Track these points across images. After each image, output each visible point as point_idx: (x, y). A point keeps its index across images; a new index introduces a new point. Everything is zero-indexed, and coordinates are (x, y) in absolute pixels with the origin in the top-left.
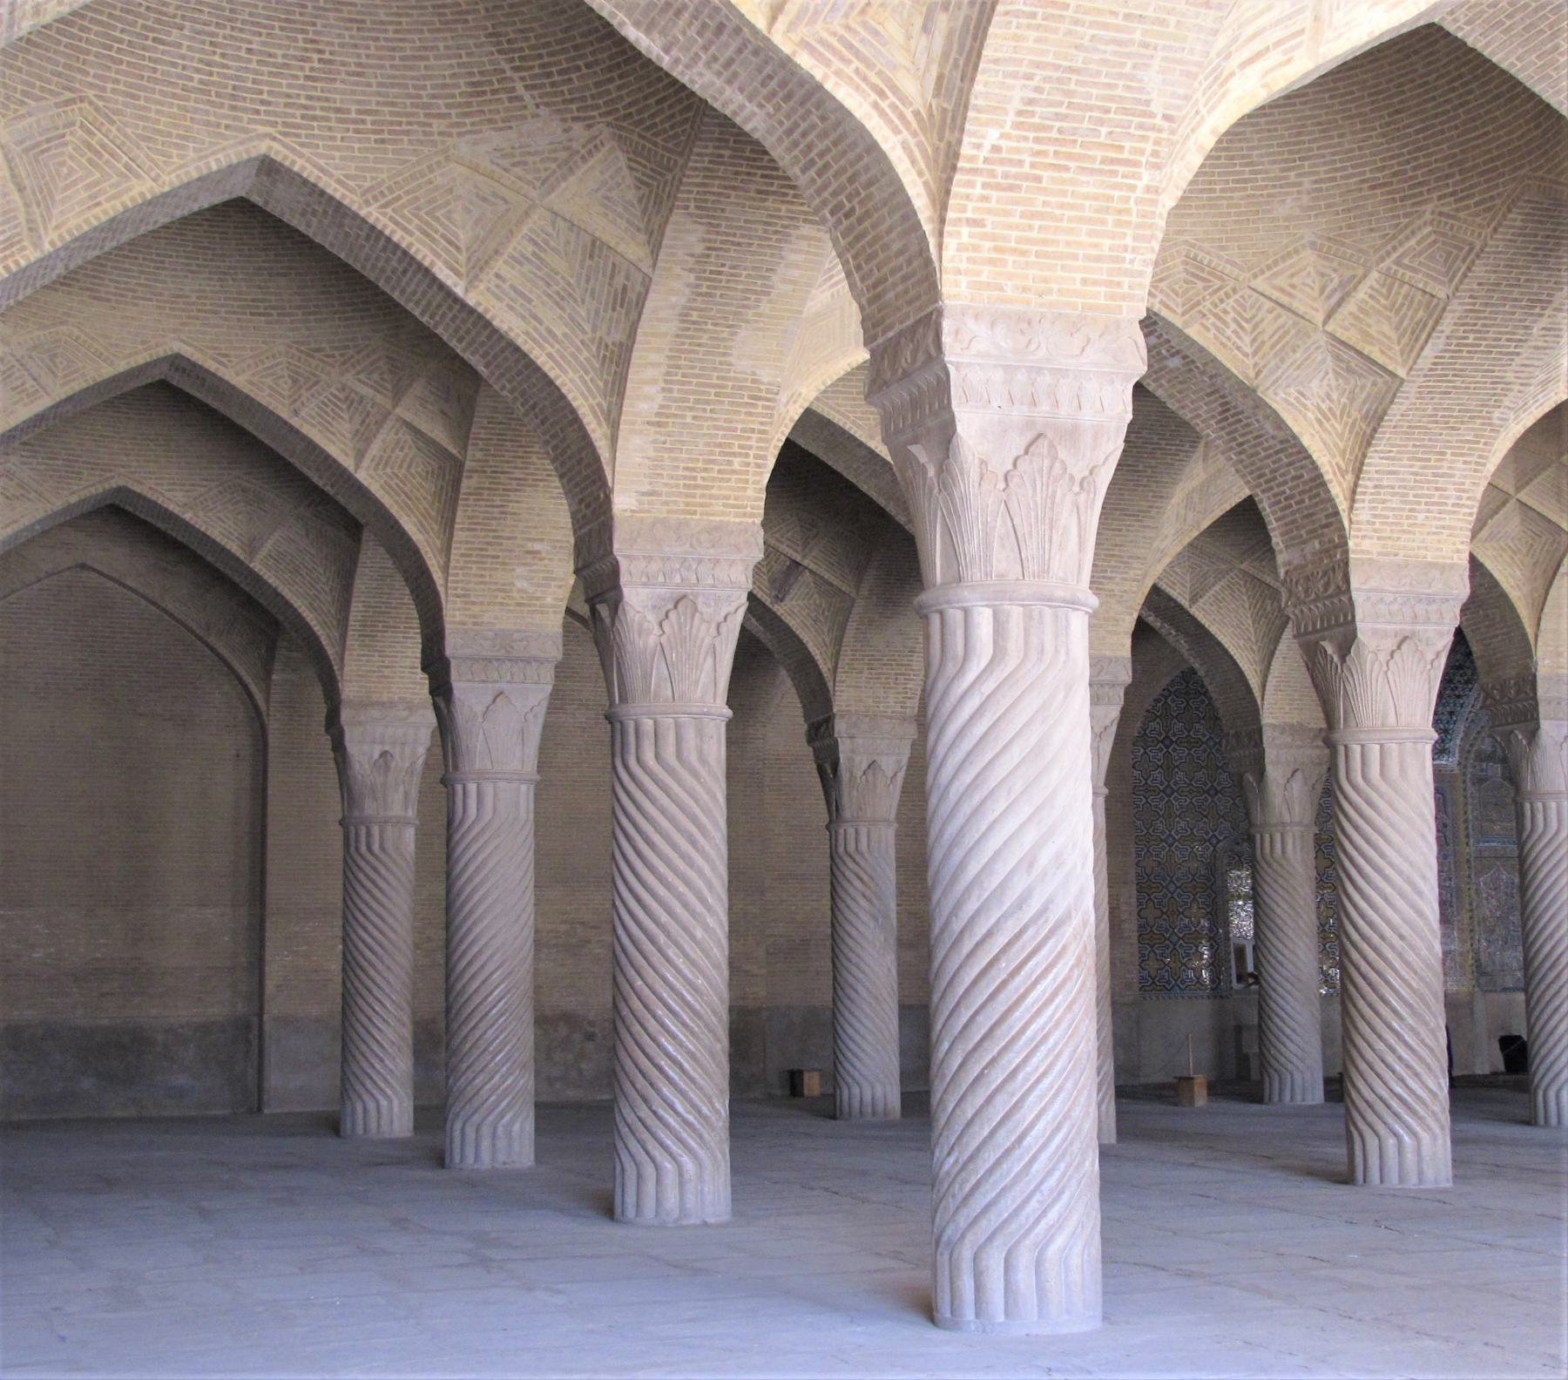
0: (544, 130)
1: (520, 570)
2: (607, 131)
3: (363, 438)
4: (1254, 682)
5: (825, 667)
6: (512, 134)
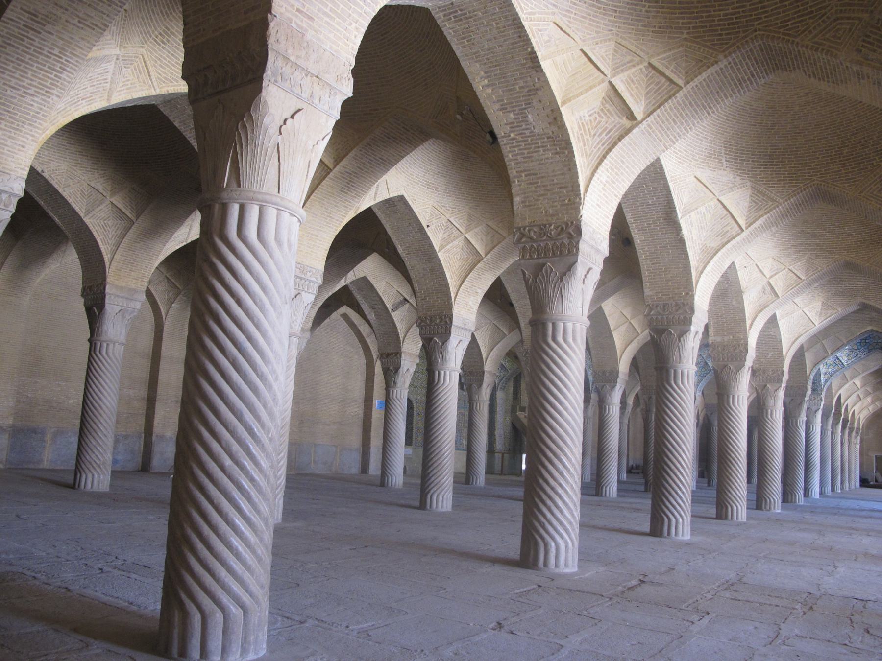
0: (726, 176)
1: (472, 298)
2: (749, 184)
3: (446, 242)
4: (484, 357)
5: (401, 336)
6: (715, 173)
